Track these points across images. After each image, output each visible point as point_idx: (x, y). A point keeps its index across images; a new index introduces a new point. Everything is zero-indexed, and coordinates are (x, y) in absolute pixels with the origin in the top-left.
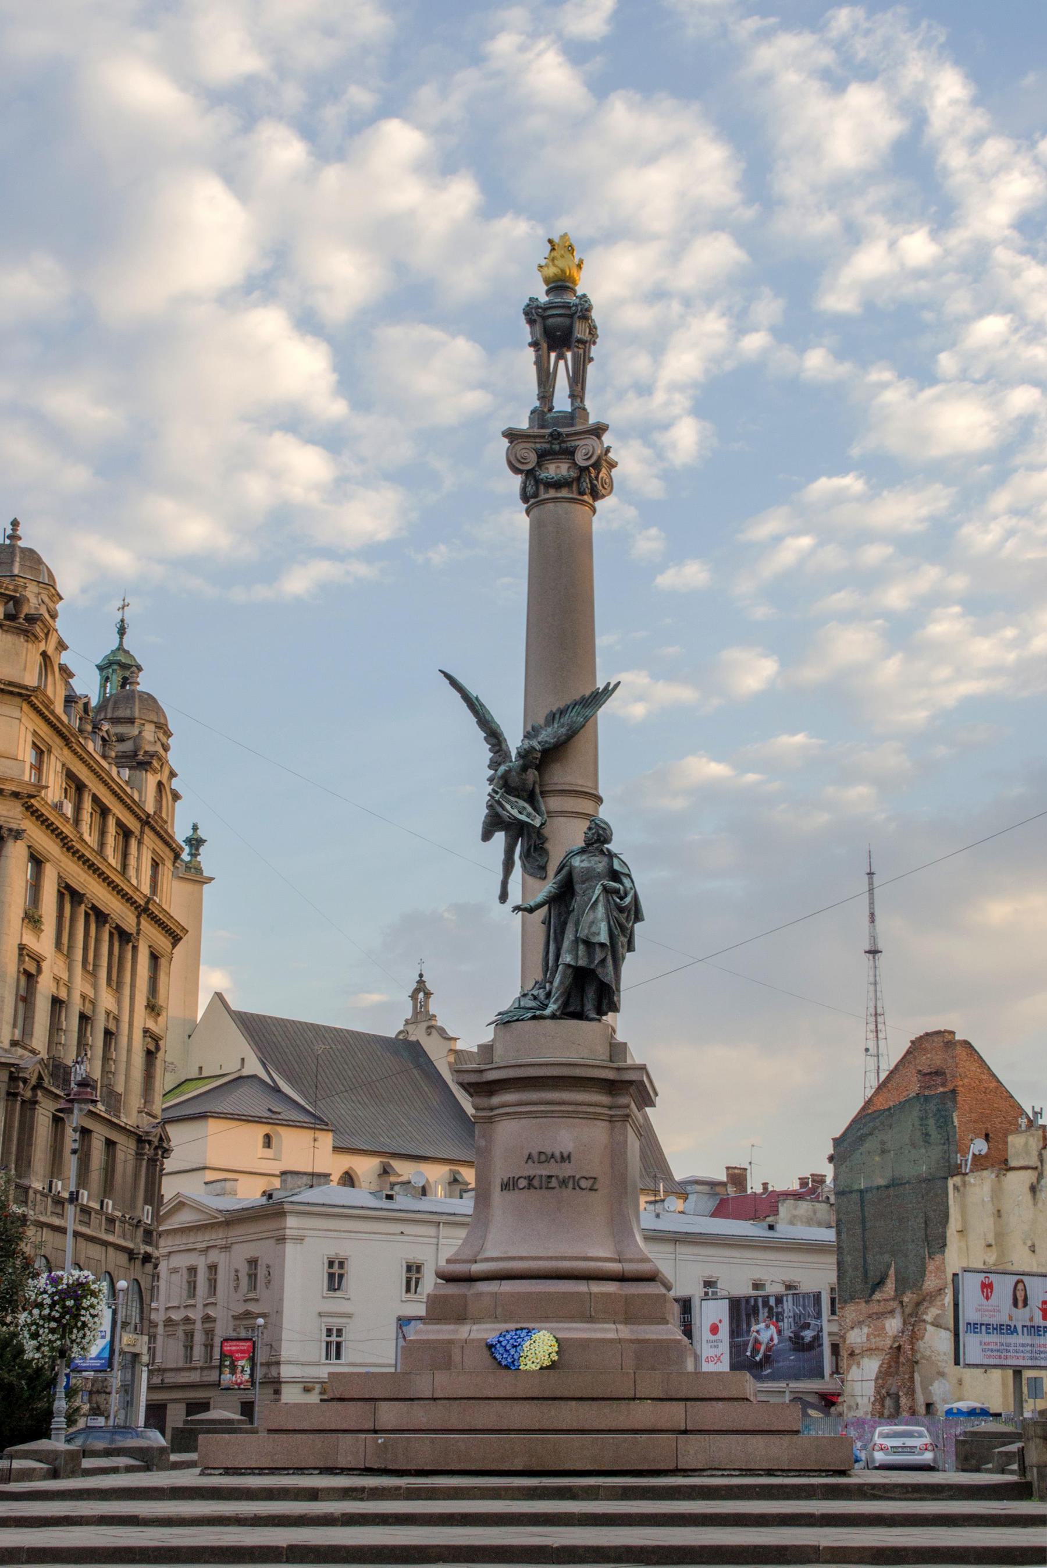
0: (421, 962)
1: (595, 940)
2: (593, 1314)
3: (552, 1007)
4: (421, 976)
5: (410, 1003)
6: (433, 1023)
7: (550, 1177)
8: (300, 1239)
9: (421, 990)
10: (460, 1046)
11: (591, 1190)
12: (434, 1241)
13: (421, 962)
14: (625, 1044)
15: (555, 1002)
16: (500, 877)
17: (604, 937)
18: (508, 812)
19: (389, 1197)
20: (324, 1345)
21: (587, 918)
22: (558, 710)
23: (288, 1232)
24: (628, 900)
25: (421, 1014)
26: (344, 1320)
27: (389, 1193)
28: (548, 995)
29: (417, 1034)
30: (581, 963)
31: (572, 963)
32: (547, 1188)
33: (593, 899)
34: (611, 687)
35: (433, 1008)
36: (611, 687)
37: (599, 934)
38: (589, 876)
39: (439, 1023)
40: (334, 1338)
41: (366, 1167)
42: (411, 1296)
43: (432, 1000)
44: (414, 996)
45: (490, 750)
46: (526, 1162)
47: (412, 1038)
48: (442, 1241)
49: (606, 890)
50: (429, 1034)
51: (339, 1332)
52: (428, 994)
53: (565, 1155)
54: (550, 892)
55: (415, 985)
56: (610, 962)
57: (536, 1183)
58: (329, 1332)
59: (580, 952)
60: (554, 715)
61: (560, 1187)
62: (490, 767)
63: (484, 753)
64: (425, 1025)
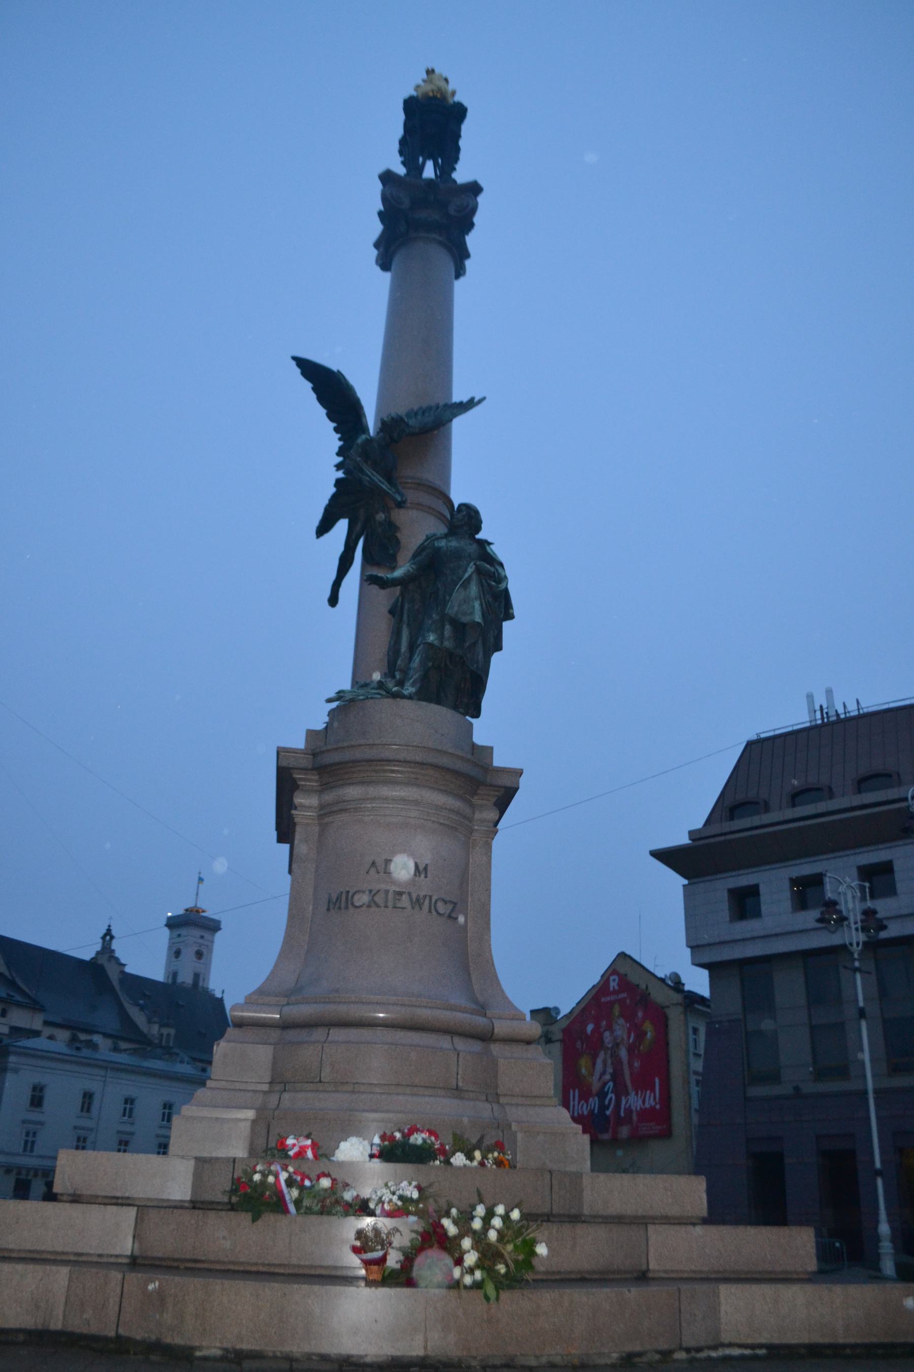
0: (111, 918)
1: (465, 619)
2: (460, 1084)
3: (409, 689)
4: (109, 926)
5: (101, 941)
6: (113, 954)
7: (400, 894)
8: (16, 1071)
9: (108, 935)
10: (128, 970)
11: (450, 917)
12: (104, 1079)
13: (111, 918)
14: (492, 748)
15: (413, 685)
16: (333, 575)
17: (478, 618)
18: (370, 477)
19: (78, 1049)
20: (23, 1142)
21: (458, 595)
22: (421, 408)
23: (10, 1065)
24: (503, 586)
25: (107, 949)
26: (39, 1127)
27: (78, 1046)
28: (401, 683)
29: (103, 961)
30: (447, 644)
31: (436, 643)
32: (394, 907)
33: (467, 575)
34: (476, 400)
35: (115, 945)
36: (476, 400)
37: (472, 613)
38: (457, 555)
39: (117, 954)
40: (30, 1139)
41: (63, 1035)
42: (85, 1114)
43: (114, 941)
44: (103, 938)
45: (340, 439)
46: (367, 873)
47: (100, 962)
48: (108, 1080)
49: (478, 571)
50: (109, 961)
51: (35, 1134)
52: (112, 937)
53: (421, 868)
54: (409, 571)
55: (104, 931)
56: (480, 649)
57: (379, 899)
58: (27, 1134)
59: (446, 633)
60: (416, 414)
61: (413, 908)
62: (338, 454)
63: (334, 442)
64: (107, 955)
